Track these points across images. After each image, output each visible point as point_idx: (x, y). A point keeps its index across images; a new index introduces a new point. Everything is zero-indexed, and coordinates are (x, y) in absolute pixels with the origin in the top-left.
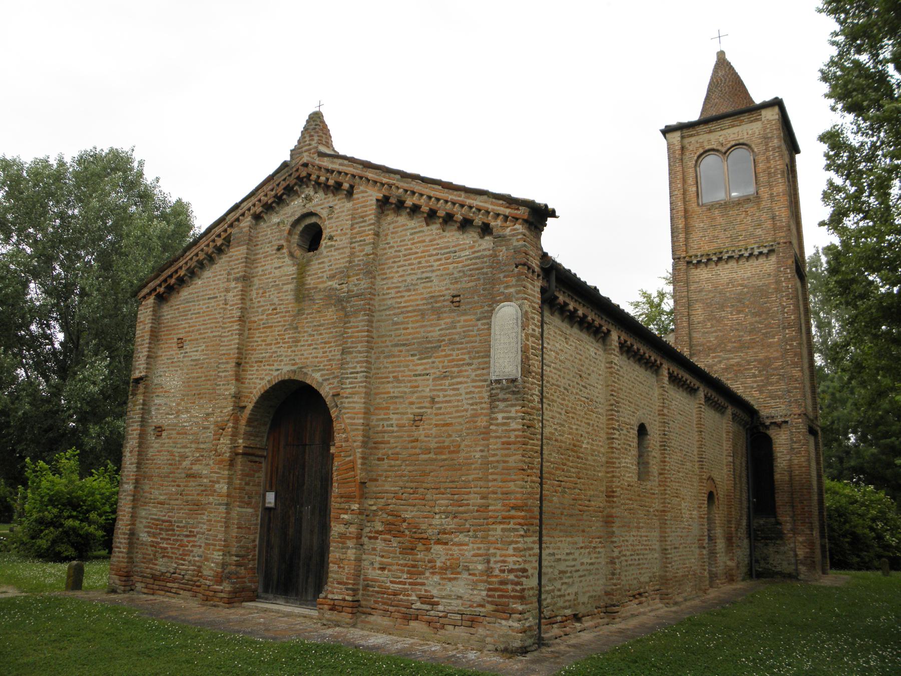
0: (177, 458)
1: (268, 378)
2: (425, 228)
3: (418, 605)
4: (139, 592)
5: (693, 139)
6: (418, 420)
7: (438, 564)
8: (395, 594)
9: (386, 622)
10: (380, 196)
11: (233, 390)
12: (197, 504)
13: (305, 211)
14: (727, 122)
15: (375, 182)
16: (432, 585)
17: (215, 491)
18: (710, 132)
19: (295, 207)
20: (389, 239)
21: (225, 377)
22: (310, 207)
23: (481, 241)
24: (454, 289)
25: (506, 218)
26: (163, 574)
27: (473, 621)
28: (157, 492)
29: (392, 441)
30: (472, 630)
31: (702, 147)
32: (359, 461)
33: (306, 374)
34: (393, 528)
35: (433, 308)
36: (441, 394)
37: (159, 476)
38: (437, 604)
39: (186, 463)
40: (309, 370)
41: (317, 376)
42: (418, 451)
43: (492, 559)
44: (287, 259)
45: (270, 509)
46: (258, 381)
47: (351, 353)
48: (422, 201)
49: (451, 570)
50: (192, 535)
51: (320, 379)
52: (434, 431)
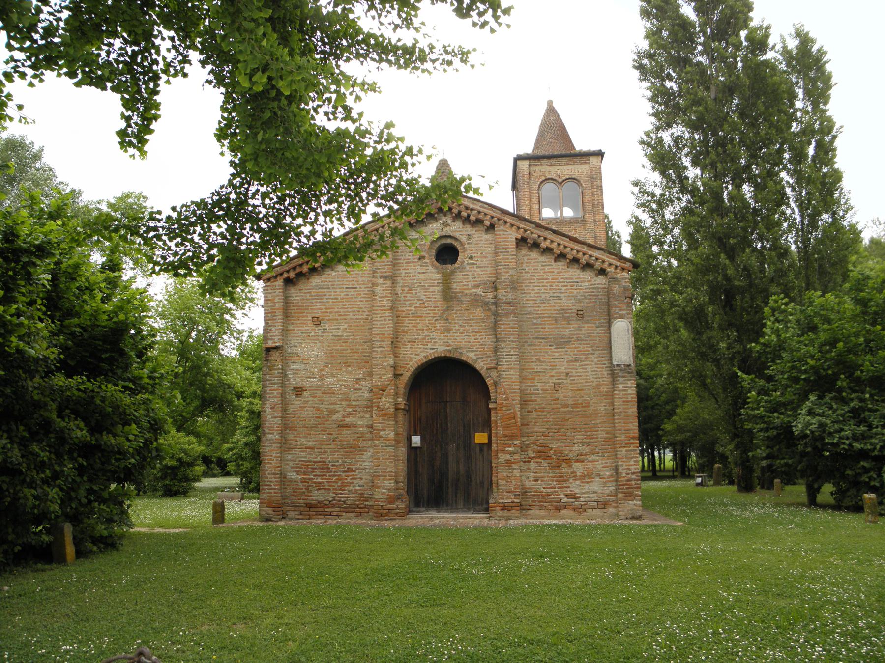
0: (326, 413)
1: (423, 354)
2: (553, 263)
3: (566, 500)
4: (290, 519)
5: (537, 168)
6: (557, 387)
7: (578, 474)
8: (548, 495)
9: (543, 513)
10: (519, 237)
11: (392, 362)
12: (355, 447)
13: (444, 233)
14: (565, 160)
15: (512, 225)
16: (575, 487)
17: (381, 437)
18: (551, 165)
19: (434, 230)
20: (524, 265)
21: (381, 351)
22: (447, 231)
23: (595, 278)
24: (578, 306)
25: (616, 267)
26: (319, 502)
27: (605, 505)
28: (304, 440)
29: (539, 399)
30: (605, 510)
31: (545, 176)
32: (519, 413)
33: (461, 353)
34: (543, 453)
35: (563, 316)
36: (574, 371)
37: (304, 427)
38: (579, 497)
39: (337, 417)
41: (472, 355)
42: (559, 406)
43: (621, 468)
44: (430, 268)
45: (416, 448)
46: (413, 356)
47: (505, 342)
48: (554, 245)
49: (588, 477)
50: (349, 470)
51: (475, 358)
52: (570, 394)
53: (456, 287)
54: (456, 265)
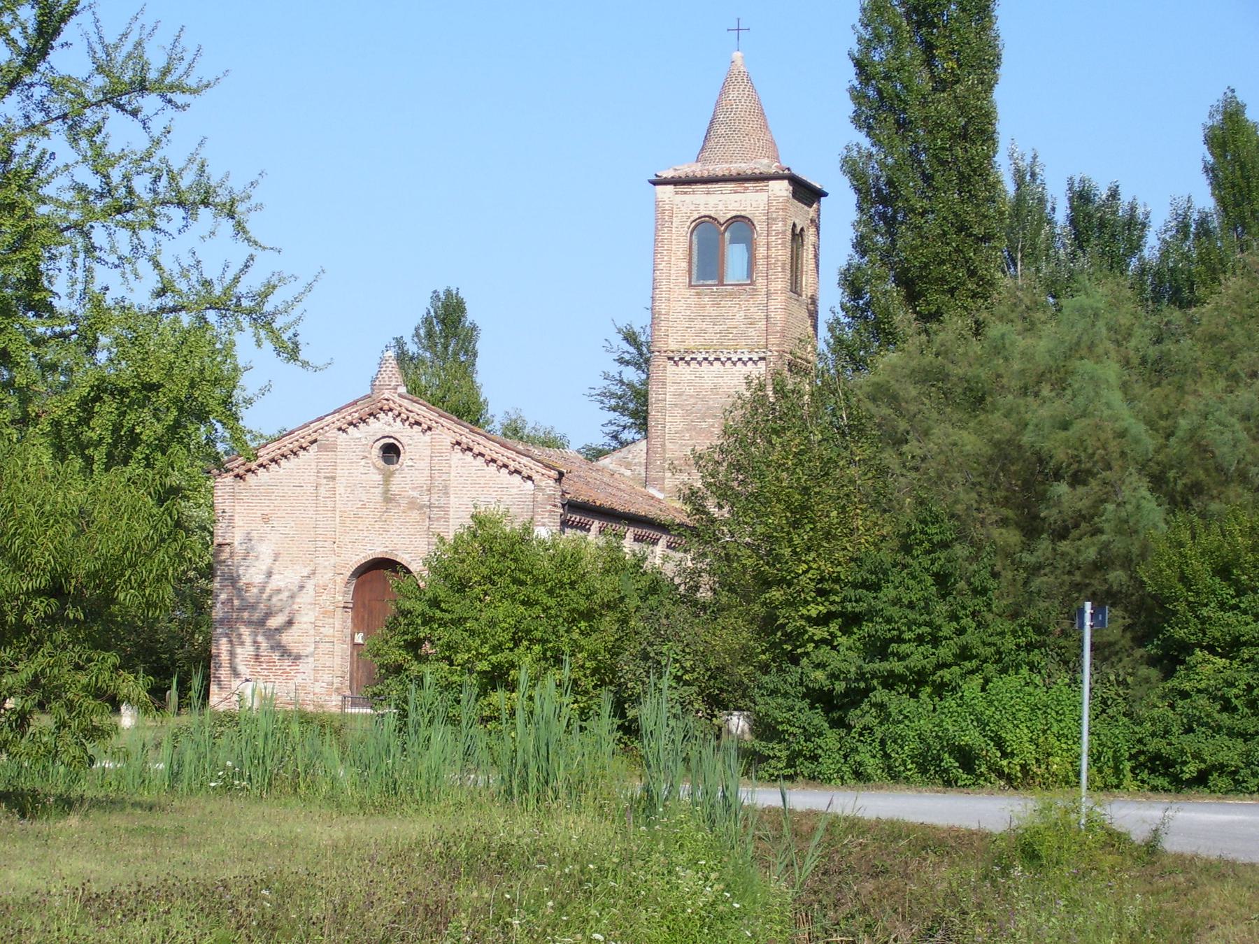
14: (730, 186)
22: (388, 430)
40: (399, 553)
41: (406, 556)
53: (394, 489)
54: (397, 466)
